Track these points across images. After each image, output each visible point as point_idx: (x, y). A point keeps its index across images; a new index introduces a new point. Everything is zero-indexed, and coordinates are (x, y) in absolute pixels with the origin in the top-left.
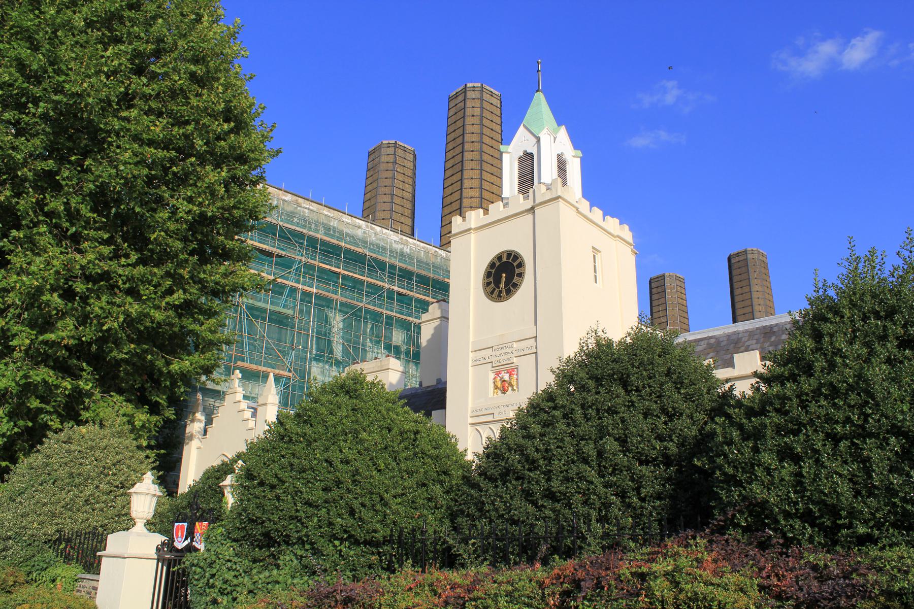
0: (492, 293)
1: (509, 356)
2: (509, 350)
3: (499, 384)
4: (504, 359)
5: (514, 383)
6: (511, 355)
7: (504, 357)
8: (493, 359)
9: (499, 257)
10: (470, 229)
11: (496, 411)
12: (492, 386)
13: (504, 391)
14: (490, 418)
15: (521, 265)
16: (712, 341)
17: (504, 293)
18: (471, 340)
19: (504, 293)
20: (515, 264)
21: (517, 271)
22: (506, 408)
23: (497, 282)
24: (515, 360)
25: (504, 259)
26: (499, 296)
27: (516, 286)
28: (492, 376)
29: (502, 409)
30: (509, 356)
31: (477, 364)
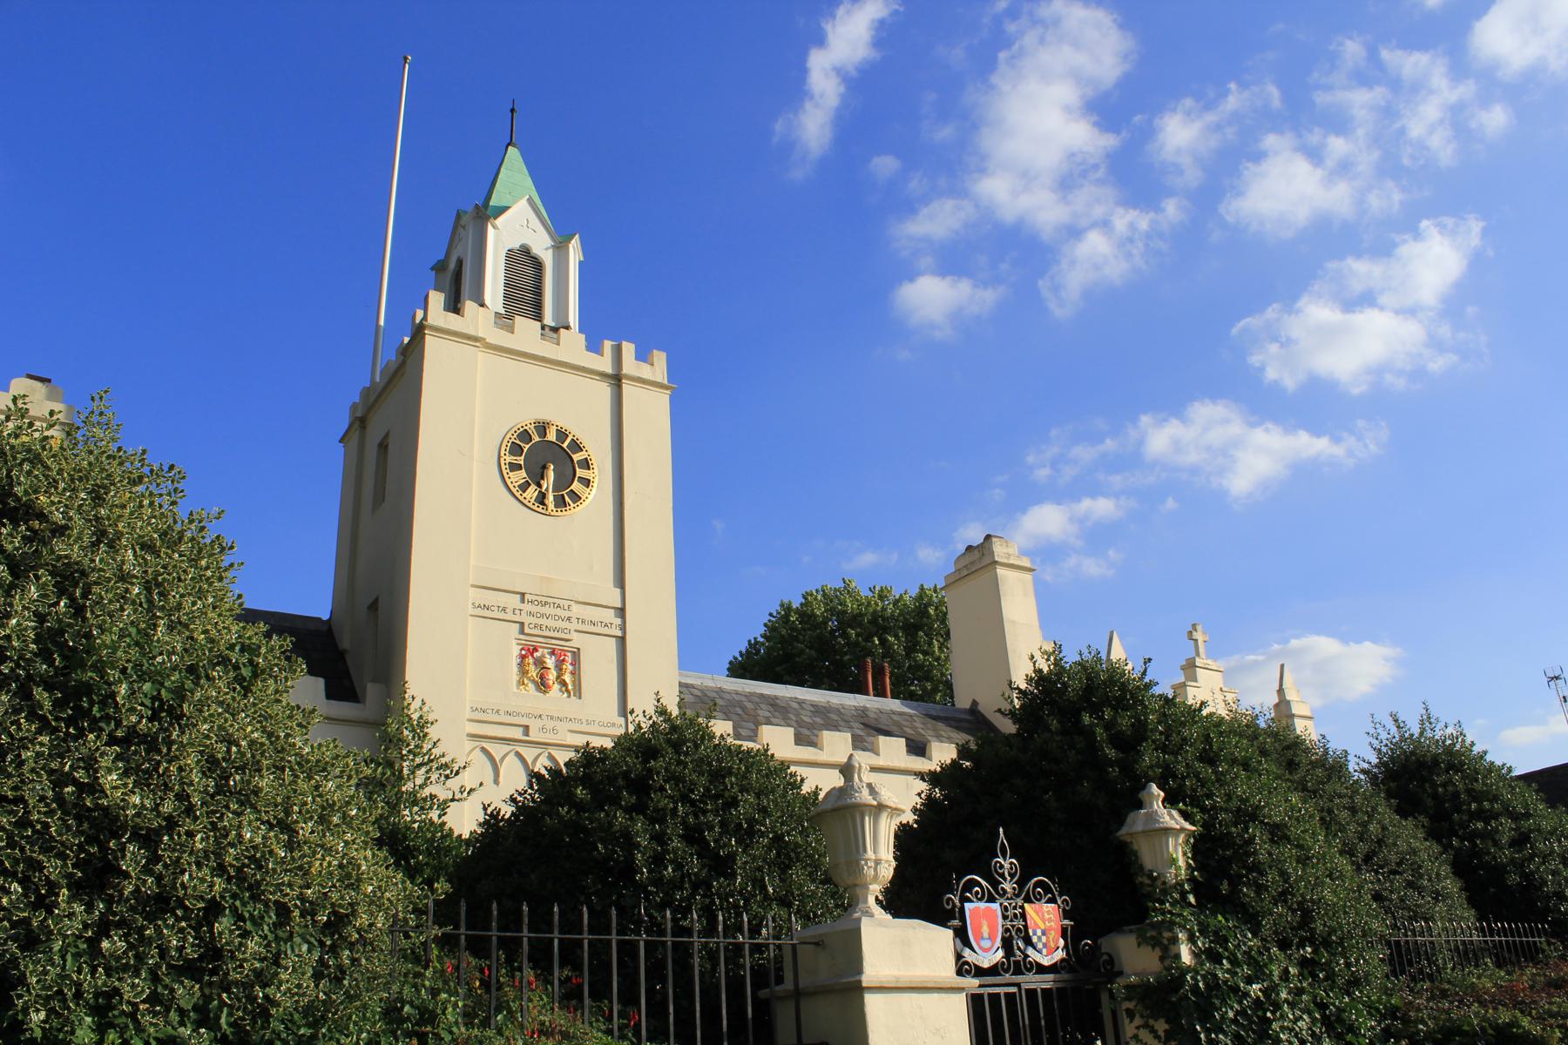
1: (560, 624)
2: (559, 612)
5: (567, 678)
8: (527, 620)
9: (542, 428)
10: (476, 339)
11: (535, 727)
12: (515, 669)
13: (542, 686)
14: (517, 733)
15: (586, 464)
17: (550, 498)
19: (550, 498)
21: (580, 472)
22: (558, 723)
23: (537, 476)
24: (574, 636)
25: (552, 436)
27: (576, 497)
28: (516, 651)
29: (550, 724)
30: (560, 624)
31: (484, 612)
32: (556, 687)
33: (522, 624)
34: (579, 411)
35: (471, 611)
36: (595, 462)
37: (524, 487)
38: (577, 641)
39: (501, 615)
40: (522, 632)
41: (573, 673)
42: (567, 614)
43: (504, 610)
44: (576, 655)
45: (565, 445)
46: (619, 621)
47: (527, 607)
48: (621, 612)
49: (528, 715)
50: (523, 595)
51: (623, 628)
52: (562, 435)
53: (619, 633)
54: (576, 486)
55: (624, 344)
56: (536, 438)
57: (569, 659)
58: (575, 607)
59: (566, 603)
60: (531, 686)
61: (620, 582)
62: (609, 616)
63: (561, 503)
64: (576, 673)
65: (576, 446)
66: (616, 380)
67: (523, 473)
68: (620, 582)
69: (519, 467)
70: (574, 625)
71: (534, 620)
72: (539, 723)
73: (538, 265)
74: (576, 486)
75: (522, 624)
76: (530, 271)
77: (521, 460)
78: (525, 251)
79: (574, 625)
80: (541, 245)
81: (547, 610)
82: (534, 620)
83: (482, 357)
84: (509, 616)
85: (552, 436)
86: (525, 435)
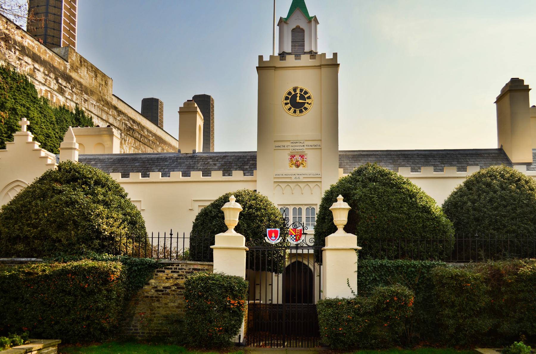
1: (301, 148)
2: (301, 144)
6: (303, 148)
7: (298, 148)
22: (300, 176)
29: (298, 176)
30: (301, 148)
36: (312, 97)
37: (289, 109)
49: (291, 175)
67: (289, 105)
69: (288, 103)
70: (305, 147)
71: (293, 148)
72: (295, 176)
77: (288, 101)
79: (305, 147)
81: (297, 144)
82: (293, 148)
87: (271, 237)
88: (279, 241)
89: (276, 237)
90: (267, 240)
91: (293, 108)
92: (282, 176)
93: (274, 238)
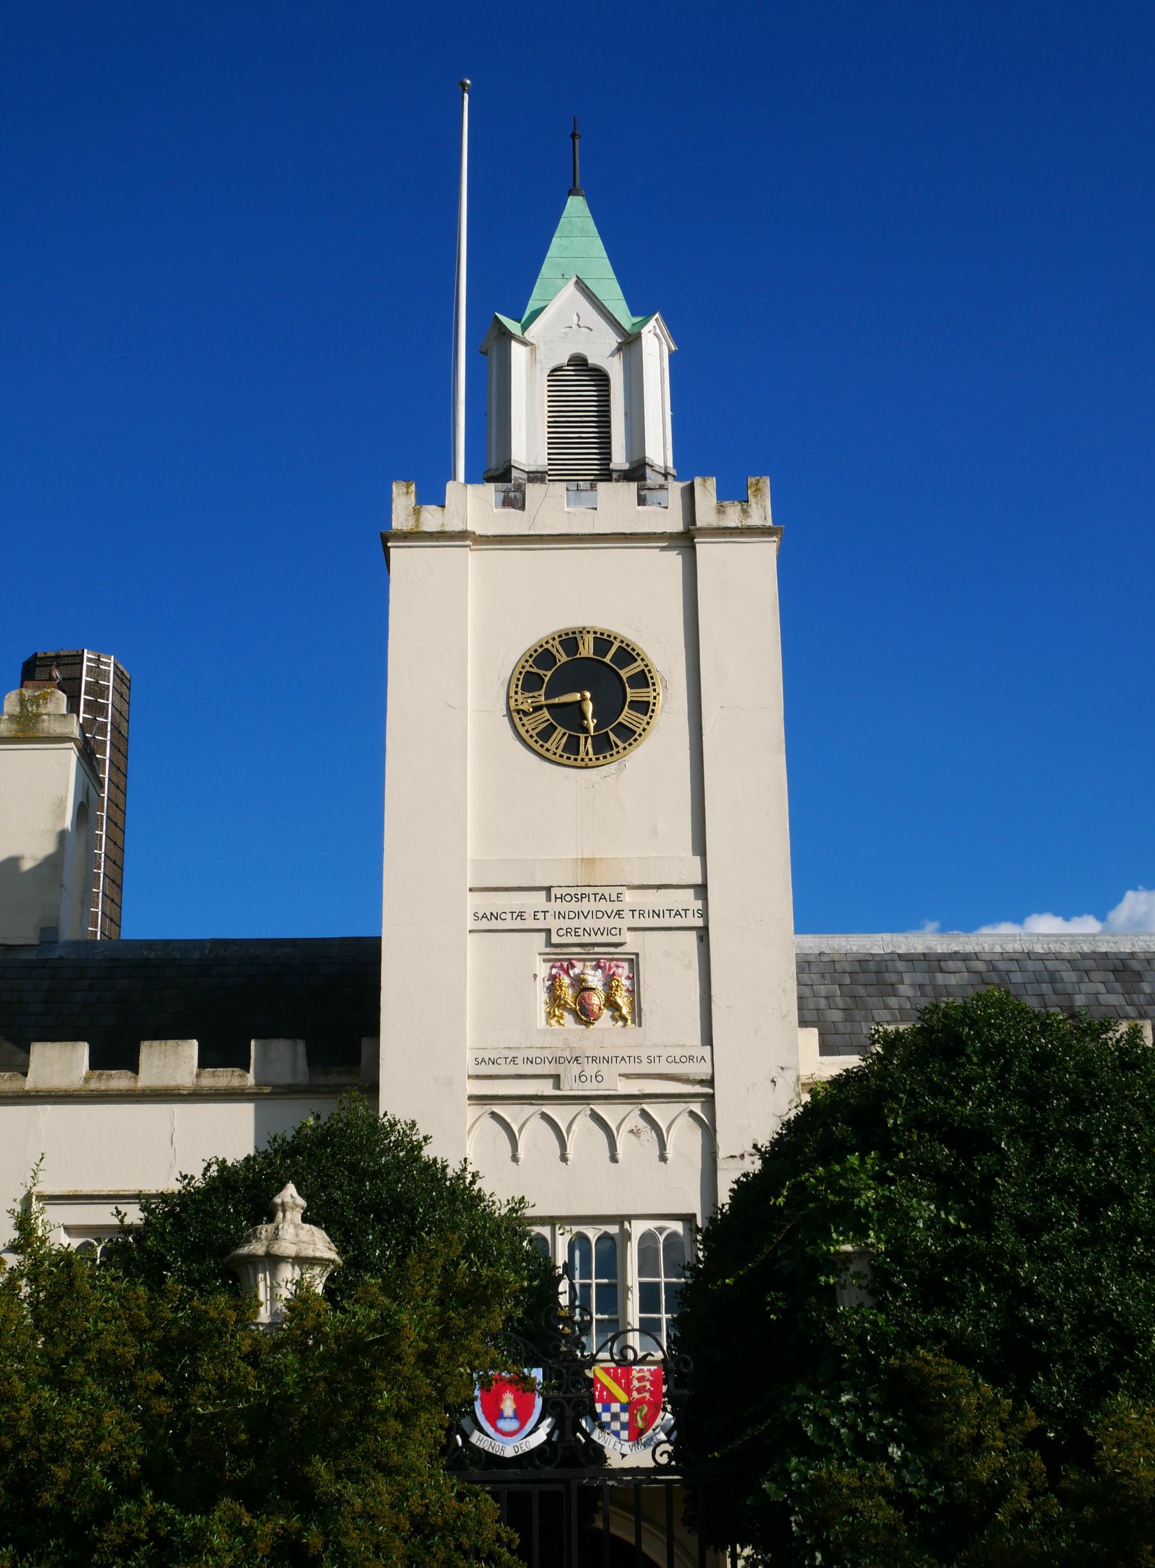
0: (545, 734)
1: (605, 923)
2: (603, 905)
3: (568, 994)
4: (591, 925)
5: (622, 999)
6: (615, 922)
7: (589, 923)
8: (553, 924)
9: (570, 641)
10: (463, 535)
12: (543, 996)
13: (584, 1015)
14: (546, 1088)
15: (642, 680)
16: (980, 966)
17: (586, 746)
18: (470, 855)
20: (625, 674)
21: (631, 694)
24: (628, 937)
25: (587, 650)
26: (572, 747)
27: (627, 733)
29: (591, 1069)
30: (605, 923)
31: (490, 925)
32: (606, 1013)
33: (548, 931)
34: (626, 599)
35: (470, 924)
38: (632, 942)
39: (518, 924)
40: (549, 943)
41: (631, 992)
42: (616, 906)
43: (521, 915)
44: (633, 962)
45: (607, 660)
46: (699, 904)
47: (559, 906)
48: (701, 890)
49: (557, 1060)
50: (548, 889)
51: (704, 914)
52: (603, 642)
53: (699, 922)
54: (626, 716)
55: (698, 481)
56: (563, 658)
57: (623, 971)
58: (629, 896)
59: (614, 891)
60: (568, 1019)
61: (700, 847)
62: (688, 899)
63: (603, 746)
64: (634, 992)
65: (627, 655)
66: (685, 541)
68: (700, 847)
71: (565, 923)
72: (575, 1069)
73: (601, 378)
74: (626, 716)
75: (548, 931)
76: (590, 392)
78: (579, 362)
79: (629, 921)
80: (601, 349)
81: (585, 906)
82: (565, 923)
83: (472, 559)
84: (530, 923)
85: (587, 650)
86: (543, 657)
87: (494, 1415)
88: (540, 1437)
89: (522, 1414)
90: (475, 1438)
91: (560, 730)
92: (512, 1070)
93: (513, 1425)
